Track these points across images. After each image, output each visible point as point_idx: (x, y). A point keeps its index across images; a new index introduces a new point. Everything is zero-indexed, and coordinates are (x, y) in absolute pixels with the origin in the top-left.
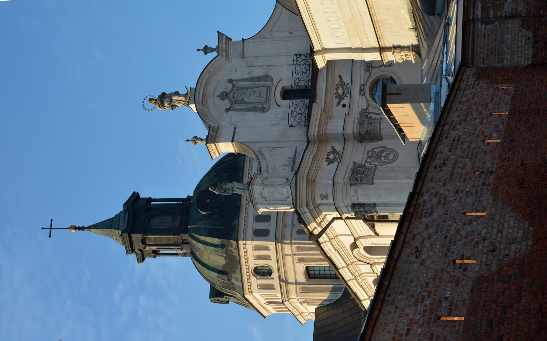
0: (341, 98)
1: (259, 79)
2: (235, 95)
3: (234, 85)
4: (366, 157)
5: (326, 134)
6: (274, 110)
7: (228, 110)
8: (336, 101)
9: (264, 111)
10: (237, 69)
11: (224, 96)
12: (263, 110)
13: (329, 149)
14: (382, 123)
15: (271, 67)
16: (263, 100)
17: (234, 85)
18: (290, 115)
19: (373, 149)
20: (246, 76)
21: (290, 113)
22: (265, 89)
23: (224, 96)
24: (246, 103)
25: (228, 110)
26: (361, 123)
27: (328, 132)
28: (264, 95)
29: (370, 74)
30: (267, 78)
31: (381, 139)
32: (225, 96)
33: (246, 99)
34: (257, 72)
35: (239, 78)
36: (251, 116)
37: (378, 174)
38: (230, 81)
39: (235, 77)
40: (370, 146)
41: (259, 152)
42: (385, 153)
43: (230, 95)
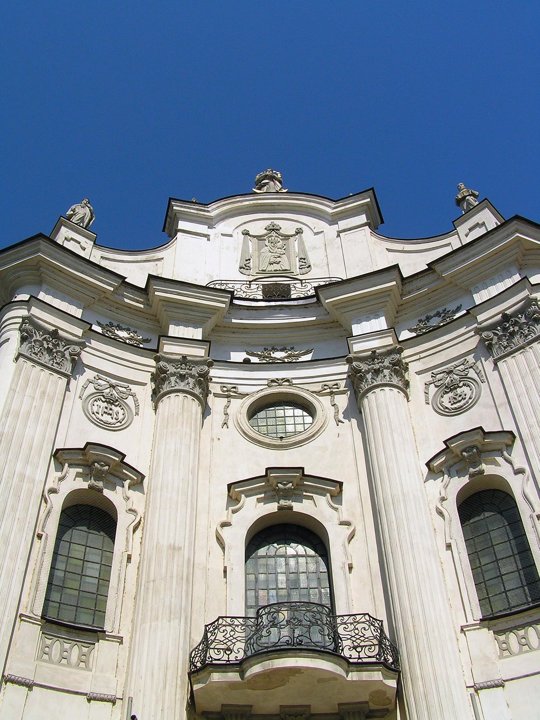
2: (273, 238)
3: (292, 236)
4: (113, 381)
7: (246, 233)
9: (241, 268)
11: (273, 229)
12: (244, 267)
14: (181, 395)
15: (326, 267)
17: (292, 236)
18: (220, 282)
19: (134, 396)
21: (223, 282)
23: (273, 229)
25: (246, 233)
29: (318, 393)
32: (271, 227)
35: (304, 239)
38: (299, 232)
39: (307, 234)
41: (154, 256)
42: (121, 412)
43: (273, 234)
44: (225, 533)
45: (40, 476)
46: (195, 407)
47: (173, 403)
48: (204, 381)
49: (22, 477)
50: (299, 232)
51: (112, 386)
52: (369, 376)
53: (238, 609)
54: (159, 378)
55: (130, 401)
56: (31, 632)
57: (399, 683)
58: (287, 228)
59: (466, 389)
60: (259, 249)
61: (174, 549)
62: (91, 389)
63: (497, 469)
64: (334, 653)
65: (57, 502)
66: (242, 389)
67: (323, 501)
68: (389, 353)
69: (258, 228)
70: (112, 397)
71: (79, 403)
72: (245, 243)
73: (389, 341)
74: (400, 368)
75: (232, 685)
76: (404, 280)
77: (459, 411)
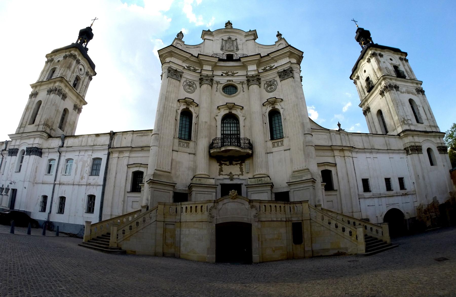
0: (226, 74)
1: (237, 47)
4: (190, 81)
5: (203, 65)
6: (222, 52)
8: (225, 72)
10: (241, 40)
11: (230, 38)
12: (222, 49)
13: (197, 68)
16: (227, 49)
20: (238, 44)
22: (232, 49)
23: (230, 38)
24: (226, 44)
25: (223, 39)
26: (207, 76)
27: (204, 66)
28: (230, 49)
30: (237, 49)
31: (200, 87)
33: (227, 44)
34: (240, 47)
36: (219, 46)
37: (174, 81)
38: (236, 39)
40: (198, 84)
44: (217, 118)
45: (175, 106)
46: (210, 87)
47: (205, 87)
48: (212, 80)
49: (171, 107)
50: (236, 39)
51: (190, 82)
52: (251, 81)
53: (219, 136)
54: (201, 80)
55: (194, 86)
56: (177, 141)
57: (252, 151)
58: (233, 38)
59: (273, 87)
60: (226, 44)
61: (206, 122)
62: (185, 83)
63: (278, 107)
64: (239, 146)
65: (179, 112)
66: (221, 82)
67: (239, 111)
68: (256, 76)
69: (226, 38)
70: (190, 85)
71: (182, 87)
72: (222, 42)
73: (257, 73)
74: (259, 79)
75: (219, 152)
76: (261, 57)
77: (271, 92)
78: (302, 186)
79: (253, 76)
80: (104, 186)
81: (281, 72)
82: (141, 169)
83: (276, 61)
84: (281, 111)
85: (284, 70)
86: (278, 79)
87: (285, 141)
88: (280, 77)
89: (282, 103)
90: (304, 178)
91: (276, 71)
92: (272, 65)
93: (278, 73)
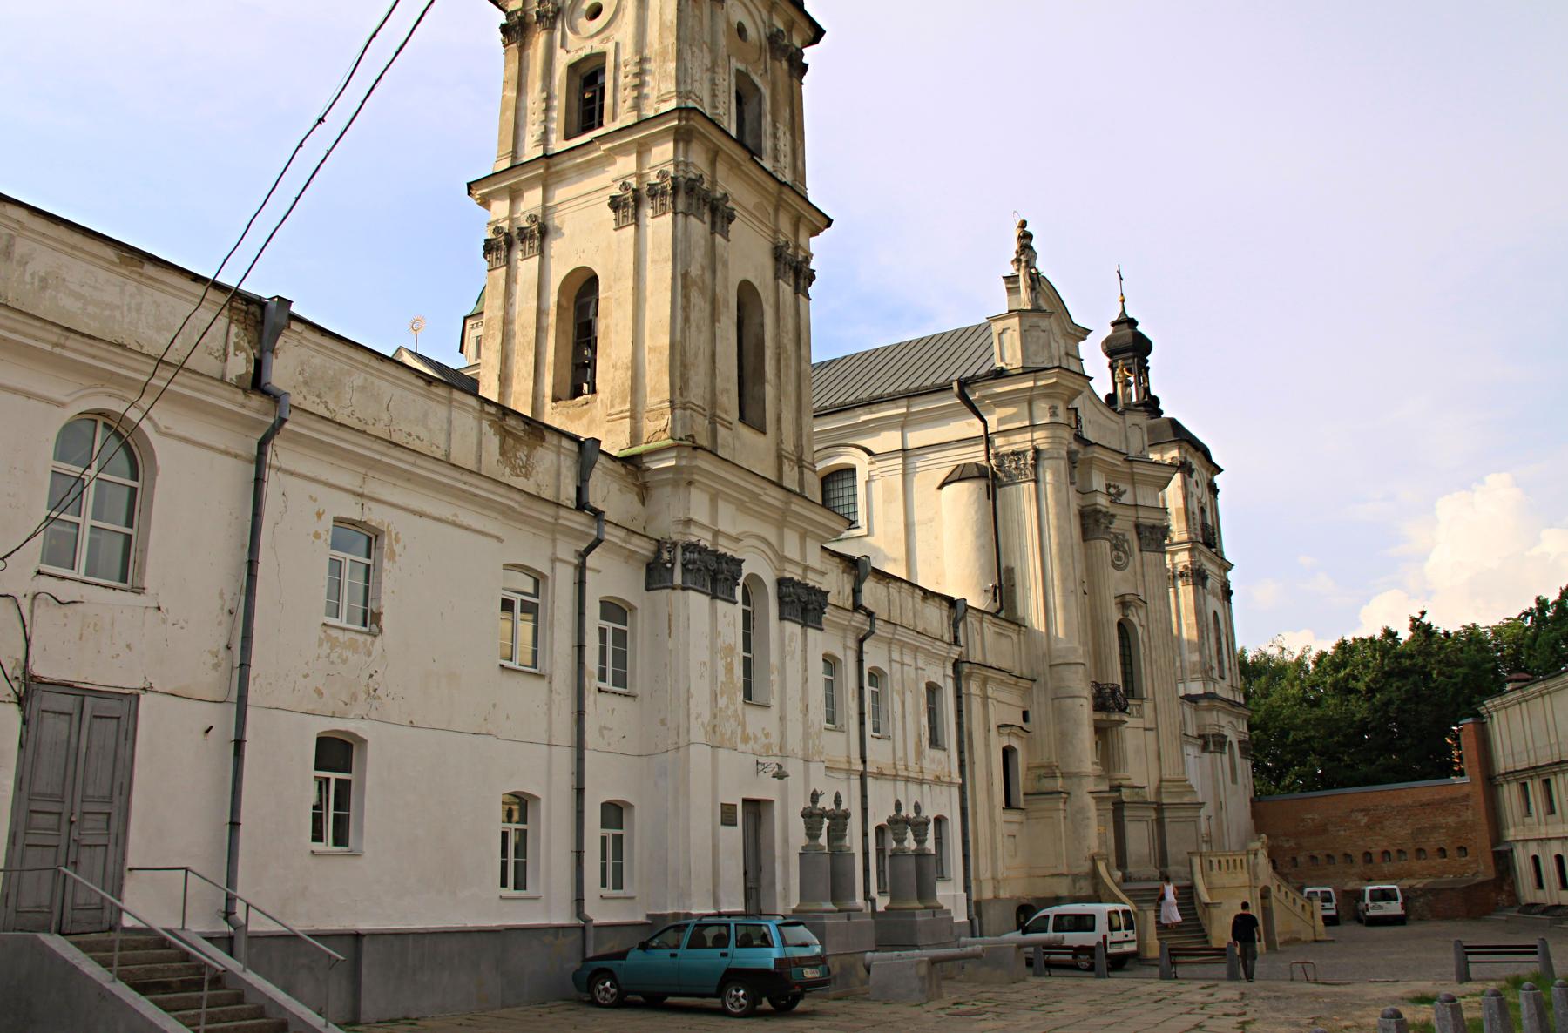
78: (1183, 814)
79: (1106, 514)
80: (962, 788)
81: (1147, 527)
82: (1015, 743)
83: (1133, 483)
84: (1140, 630)
85: (1154, 527)
86: (1132, 536)
87: (1147, 707)
88: (1140, 538)
89: (1142, 613)
90: (1186, 800)
91: (1131, 512)
92: (1122, 487)
93: (1137, 526)
